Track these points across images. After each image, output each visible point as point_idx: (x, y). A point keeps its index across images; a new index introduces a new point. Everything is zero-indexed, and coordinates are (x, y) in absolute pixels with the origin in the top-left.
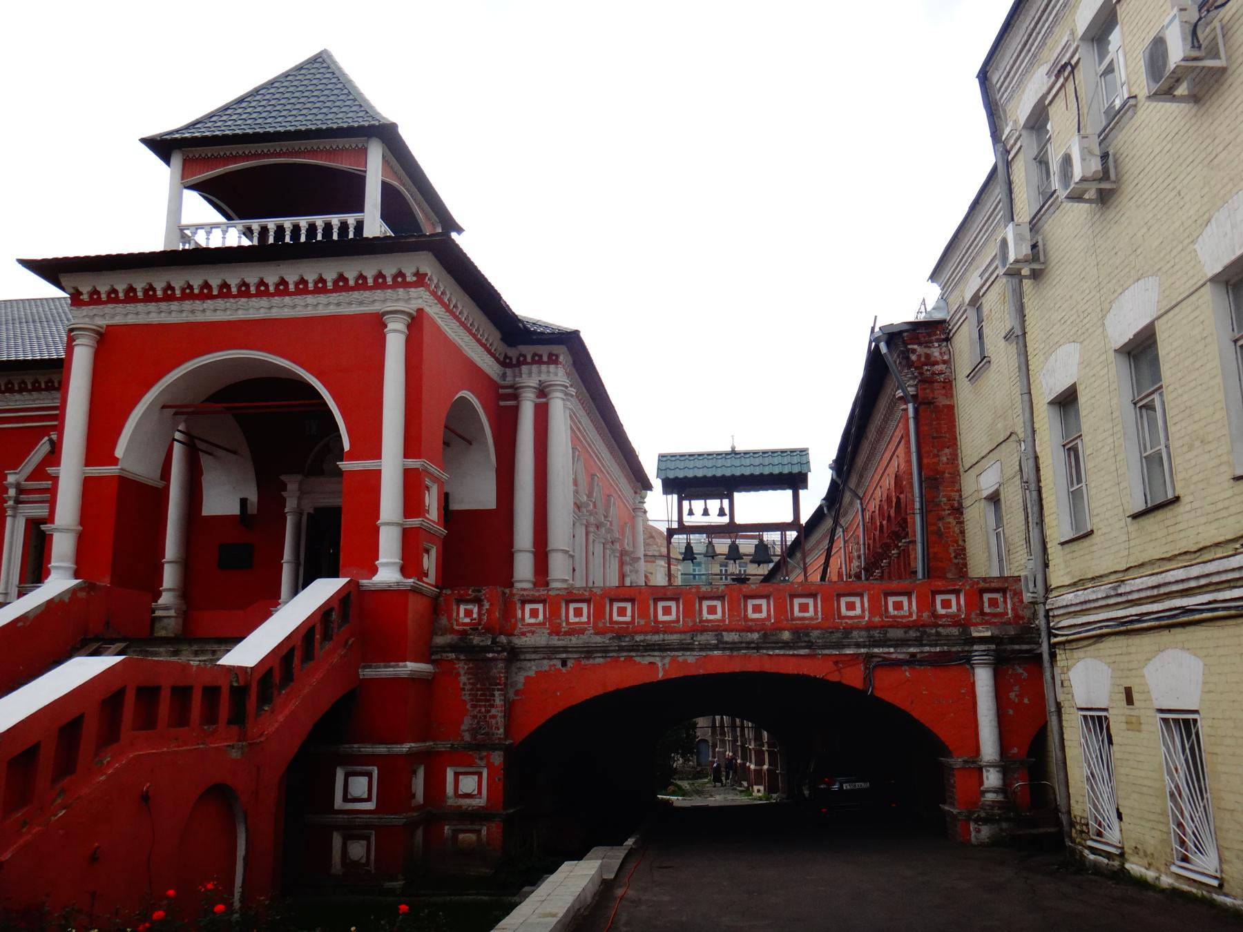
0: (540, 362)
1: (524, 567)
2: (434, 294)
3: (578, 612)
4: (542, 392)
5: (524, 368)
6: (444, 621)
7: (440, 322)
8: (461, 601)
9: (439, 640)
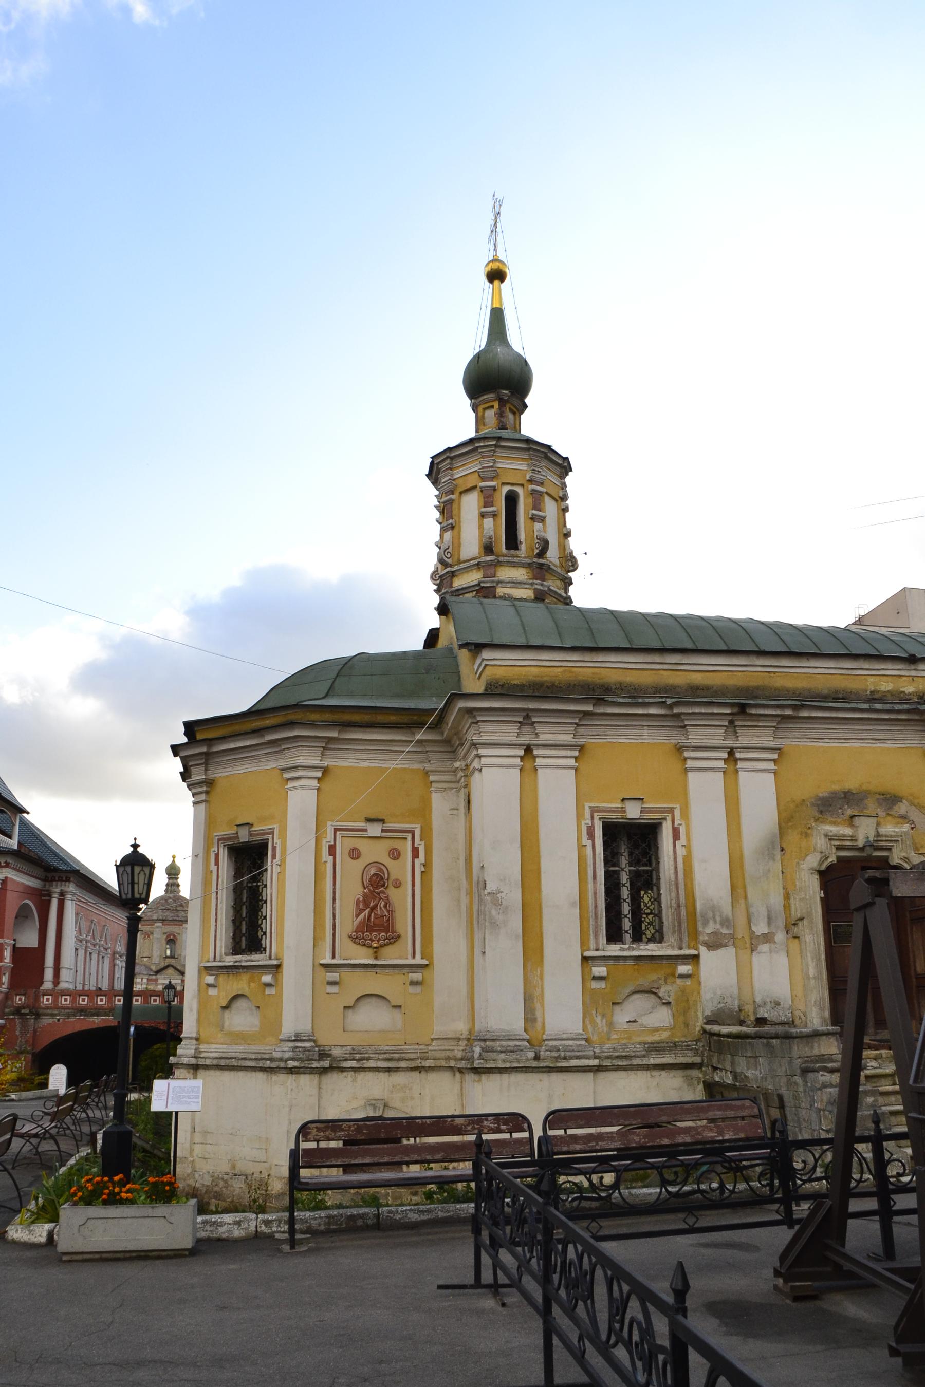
0: (62, 881)
1: (49, 974)
2: (13, 868)
3: (66, 1000)
4: (62, 894)
5: (54, 883)
6: (10, 1003)
7: (15, 878)
8: (17, 995)
9: (7, 1010)
